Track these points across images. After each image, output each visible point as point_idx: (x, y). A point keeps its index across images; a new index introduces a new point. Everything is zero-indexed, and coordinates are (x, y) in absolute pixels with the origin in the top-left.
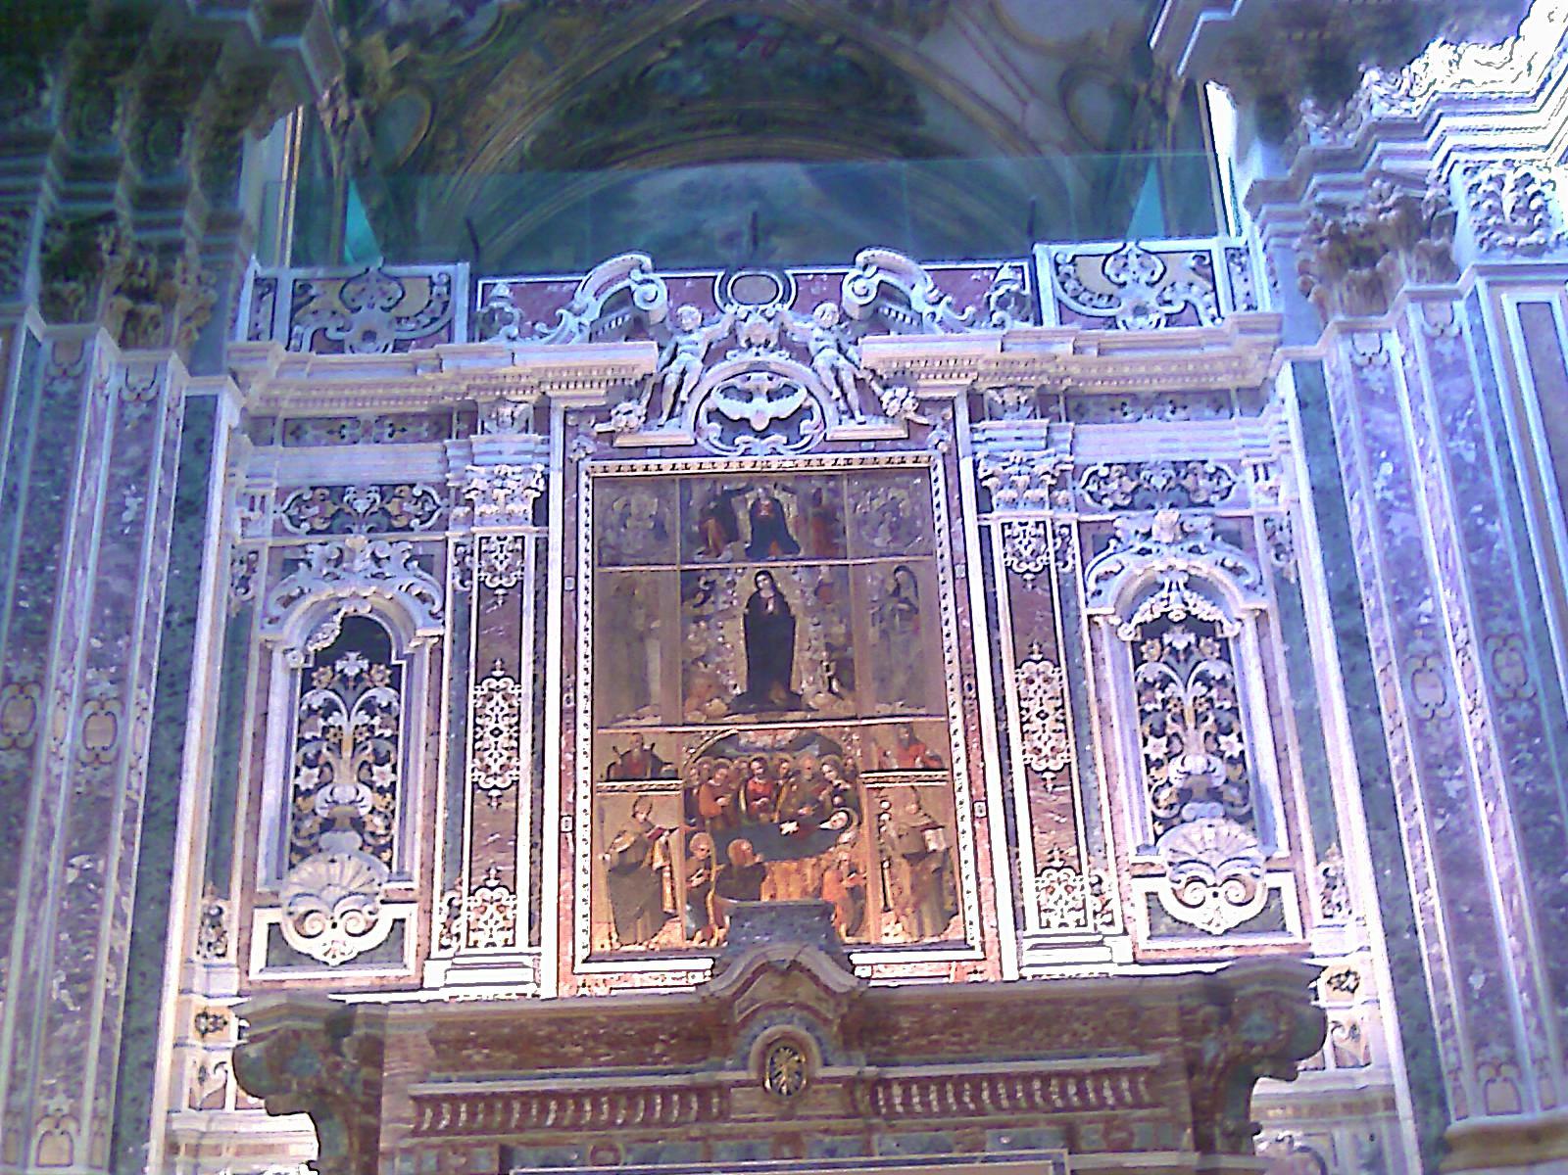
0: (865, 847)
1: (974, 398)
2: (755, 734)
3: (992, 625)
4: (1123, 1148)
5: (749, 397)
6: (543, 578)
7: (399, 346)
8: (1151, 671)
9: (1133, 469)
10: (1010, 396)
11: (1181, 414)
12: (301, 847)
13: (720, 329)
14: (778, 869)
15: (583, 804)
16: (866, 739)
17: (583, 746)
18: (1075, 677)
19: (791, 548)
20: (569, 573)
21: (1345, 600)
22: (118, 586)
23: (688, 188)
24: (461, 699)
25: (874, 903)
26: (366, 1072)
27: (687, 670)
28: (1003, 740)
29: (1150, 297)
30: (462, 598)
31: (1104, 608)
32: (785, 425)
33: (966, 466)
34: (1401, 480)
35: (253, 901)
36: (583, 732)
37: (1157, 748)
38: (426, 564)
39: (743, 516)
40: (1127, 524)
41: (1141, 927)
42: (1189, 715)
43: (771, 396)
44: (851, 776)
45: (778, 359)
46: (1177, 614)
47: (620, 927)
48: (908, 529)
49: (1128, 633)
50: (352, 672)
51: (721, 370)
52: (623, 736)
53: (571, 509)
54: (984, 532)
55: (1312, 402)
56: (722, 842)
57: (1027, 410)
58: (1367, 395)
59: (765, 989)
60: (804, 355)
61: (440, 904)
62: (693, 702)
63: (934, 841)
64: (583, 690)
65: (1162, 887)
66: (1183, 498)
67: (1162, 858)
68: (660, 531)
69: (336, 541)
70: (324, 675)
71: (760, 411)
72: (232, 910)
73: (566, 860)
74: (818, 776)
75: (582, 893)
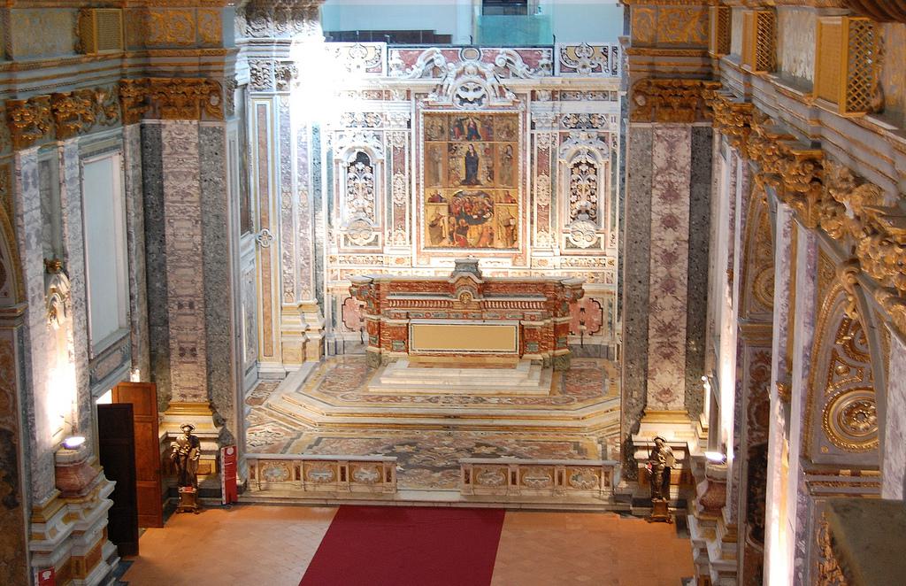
0: (495, 222)
1: (533, 92)
2: (464, 189)
3: (532, 163)
4: (533, 320)
5: (467, 90)
6: (410, 144)
8: (575, 177)
9: (577, 116)
10: (543, 93)
11: (594, 98)
13: (460, 69)
14: (472, 227)
15: (422, 209)
16: (497, 194)
17: (422, 194)
18: (553, 180)
19: (478, 137)
20: (417, 144)
22: (303, 160)
24: (389, 178)
25: (495, 237)
26: (377, 292)
27: (449, 172)
28: (532, 196)
29: (588, 62)
30: (388, 149)
32: (479, 101)
33: (528, 115)
36: (422, 190)
37: (574, 198)
39: (465, 127)
40: (573, 133)
41: (563, 245)
42: (584, 190)
43: (475, 90)
44: (492, 204)
45: (477, 78)
46: (584, 161)
47: (432, 240)
48: (511, 133)
49: (570, 166)
50: (360, 168)
51: (460, 80)
53: (417, 124)
54: (532, 135)
56: (458, 219)
57: (548, 98)
59: (461, 282)
60: (484, 76)
61: (387, 233)
62: (451, 181)
64: (422, 178)
66: (591, 126)
67: (570, 229)
68: (442, 131)
70: (352, 169)
71: (471, 95)
73: (418, 224)
74: (483, 203)
75: (422, 232)
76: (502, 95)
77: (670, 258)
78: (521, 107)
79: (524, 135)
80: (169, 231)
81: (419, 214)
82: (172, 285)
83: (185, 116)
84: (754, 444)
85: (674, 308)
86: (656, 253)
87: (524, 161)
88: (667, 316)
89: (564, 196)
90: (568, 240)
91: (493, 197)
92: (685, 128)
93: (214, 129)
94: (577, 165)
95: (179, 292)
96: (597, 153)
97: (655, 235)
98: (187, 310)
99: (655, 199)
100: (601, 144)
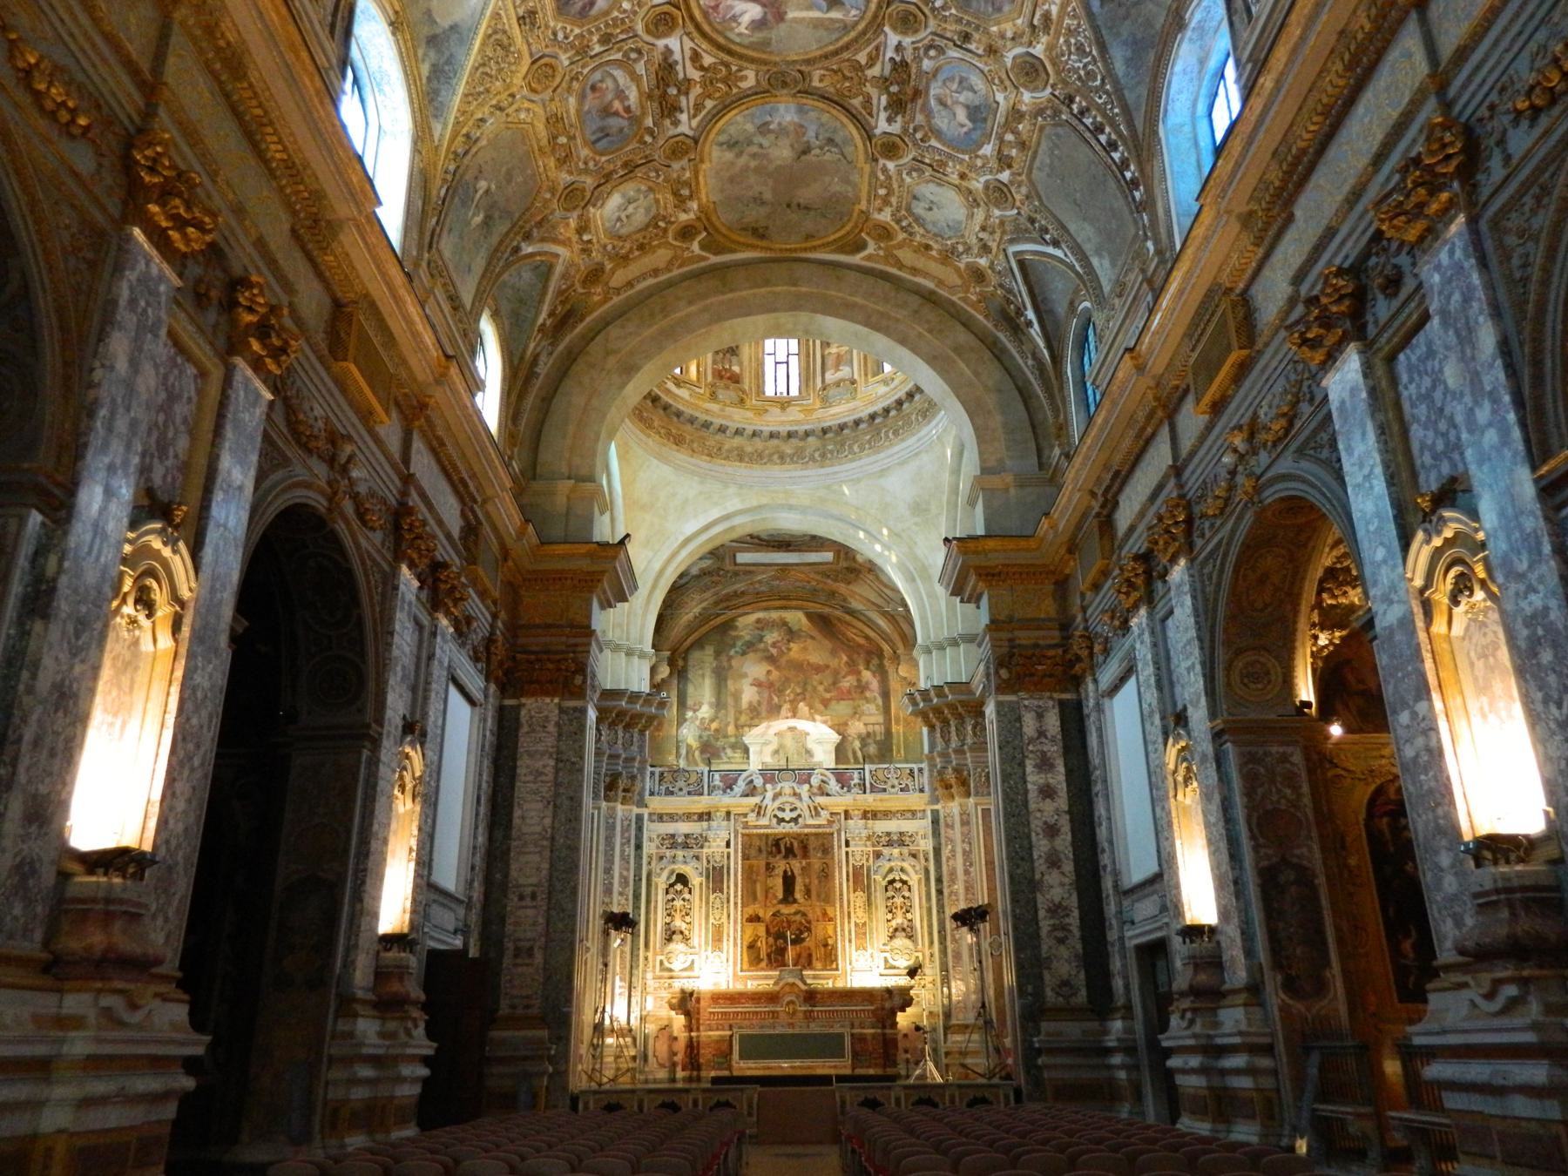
1: (846, 812)
2: (786, 910)
7: (689, 793)
8: (890, 893)
9: (888, 834)
12: (669, 940)
19: (795, 856)
21: (939, 880)
23: (758, 621)
31: (878, 878)
32: (795, 820)
34: (953, 851)
35: (655, 954)
37: (890, 916)
38: (697, 858)
40: (886, 851)
41: (882, 965)
45: (792, 799)
48: (826, 850)
49: (884, 883)
52: (750, 911)
55: (935, 822)
56: (776, 939)
58: (947, 826)
59: (787, 989)
63: (830, 942)
65: (888, 955)
66: (902, 844)
68: (760, 850)
69: (674, 852)
71: (787, 815)
72: (650, 955)
76: (818, 814)
77: (1052, 831)
78: (836, 826)
79: (840, 853)
80: (517, 813)
81: (735, 935)
82: (514, 873)
83: (547, 694)
84: (1265, 863)
85: (1062, 885)
86: (1036, 824)
87: (841, 878)
88: (1057, 894)
89: (881, 913)
90: (886, 961)
91: (810, 916)
92: (1051, 698)
93: (575, 709)
94: (892, 882)
95: (521, 881)
96: (910, 870)
97: (1032, 806)
98: (528, 902)
99: (1029, 769)
100: (912, 861)
